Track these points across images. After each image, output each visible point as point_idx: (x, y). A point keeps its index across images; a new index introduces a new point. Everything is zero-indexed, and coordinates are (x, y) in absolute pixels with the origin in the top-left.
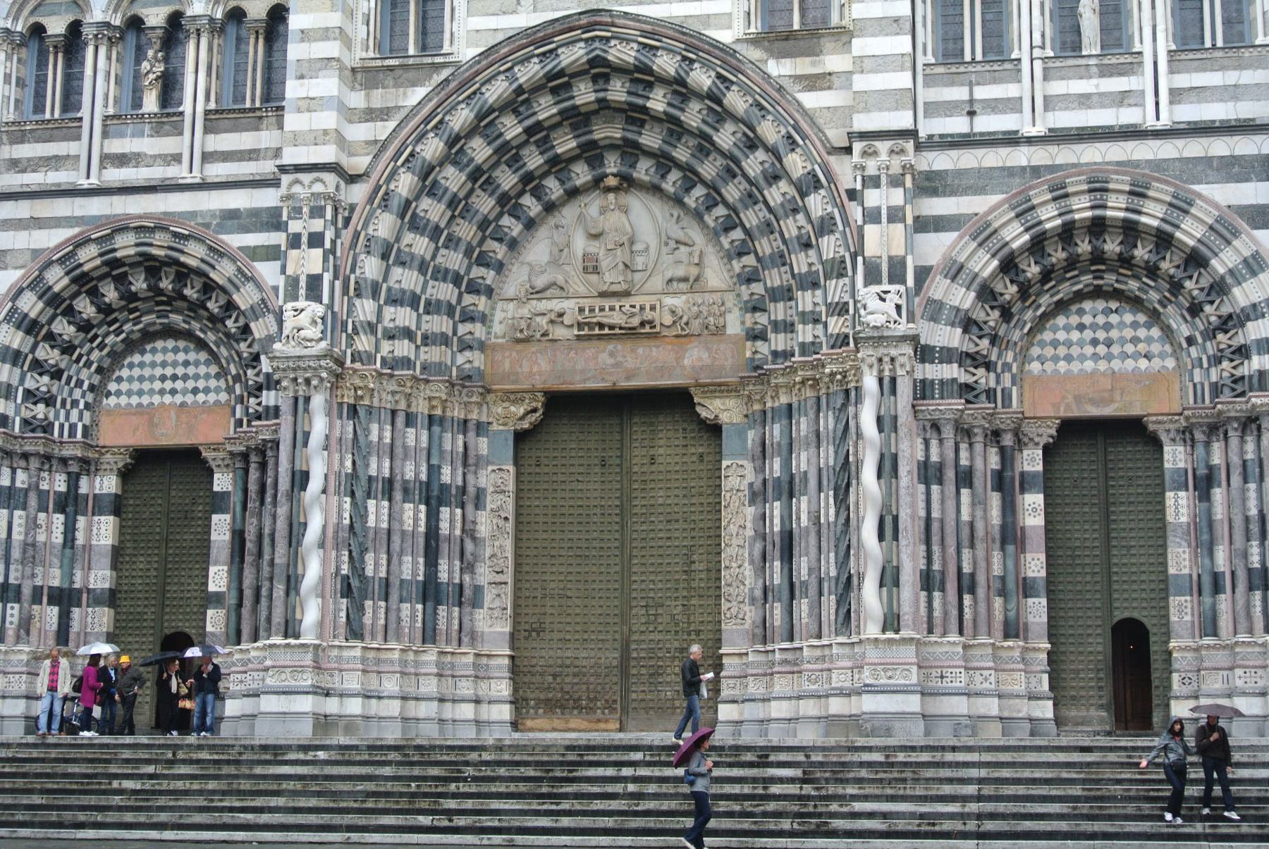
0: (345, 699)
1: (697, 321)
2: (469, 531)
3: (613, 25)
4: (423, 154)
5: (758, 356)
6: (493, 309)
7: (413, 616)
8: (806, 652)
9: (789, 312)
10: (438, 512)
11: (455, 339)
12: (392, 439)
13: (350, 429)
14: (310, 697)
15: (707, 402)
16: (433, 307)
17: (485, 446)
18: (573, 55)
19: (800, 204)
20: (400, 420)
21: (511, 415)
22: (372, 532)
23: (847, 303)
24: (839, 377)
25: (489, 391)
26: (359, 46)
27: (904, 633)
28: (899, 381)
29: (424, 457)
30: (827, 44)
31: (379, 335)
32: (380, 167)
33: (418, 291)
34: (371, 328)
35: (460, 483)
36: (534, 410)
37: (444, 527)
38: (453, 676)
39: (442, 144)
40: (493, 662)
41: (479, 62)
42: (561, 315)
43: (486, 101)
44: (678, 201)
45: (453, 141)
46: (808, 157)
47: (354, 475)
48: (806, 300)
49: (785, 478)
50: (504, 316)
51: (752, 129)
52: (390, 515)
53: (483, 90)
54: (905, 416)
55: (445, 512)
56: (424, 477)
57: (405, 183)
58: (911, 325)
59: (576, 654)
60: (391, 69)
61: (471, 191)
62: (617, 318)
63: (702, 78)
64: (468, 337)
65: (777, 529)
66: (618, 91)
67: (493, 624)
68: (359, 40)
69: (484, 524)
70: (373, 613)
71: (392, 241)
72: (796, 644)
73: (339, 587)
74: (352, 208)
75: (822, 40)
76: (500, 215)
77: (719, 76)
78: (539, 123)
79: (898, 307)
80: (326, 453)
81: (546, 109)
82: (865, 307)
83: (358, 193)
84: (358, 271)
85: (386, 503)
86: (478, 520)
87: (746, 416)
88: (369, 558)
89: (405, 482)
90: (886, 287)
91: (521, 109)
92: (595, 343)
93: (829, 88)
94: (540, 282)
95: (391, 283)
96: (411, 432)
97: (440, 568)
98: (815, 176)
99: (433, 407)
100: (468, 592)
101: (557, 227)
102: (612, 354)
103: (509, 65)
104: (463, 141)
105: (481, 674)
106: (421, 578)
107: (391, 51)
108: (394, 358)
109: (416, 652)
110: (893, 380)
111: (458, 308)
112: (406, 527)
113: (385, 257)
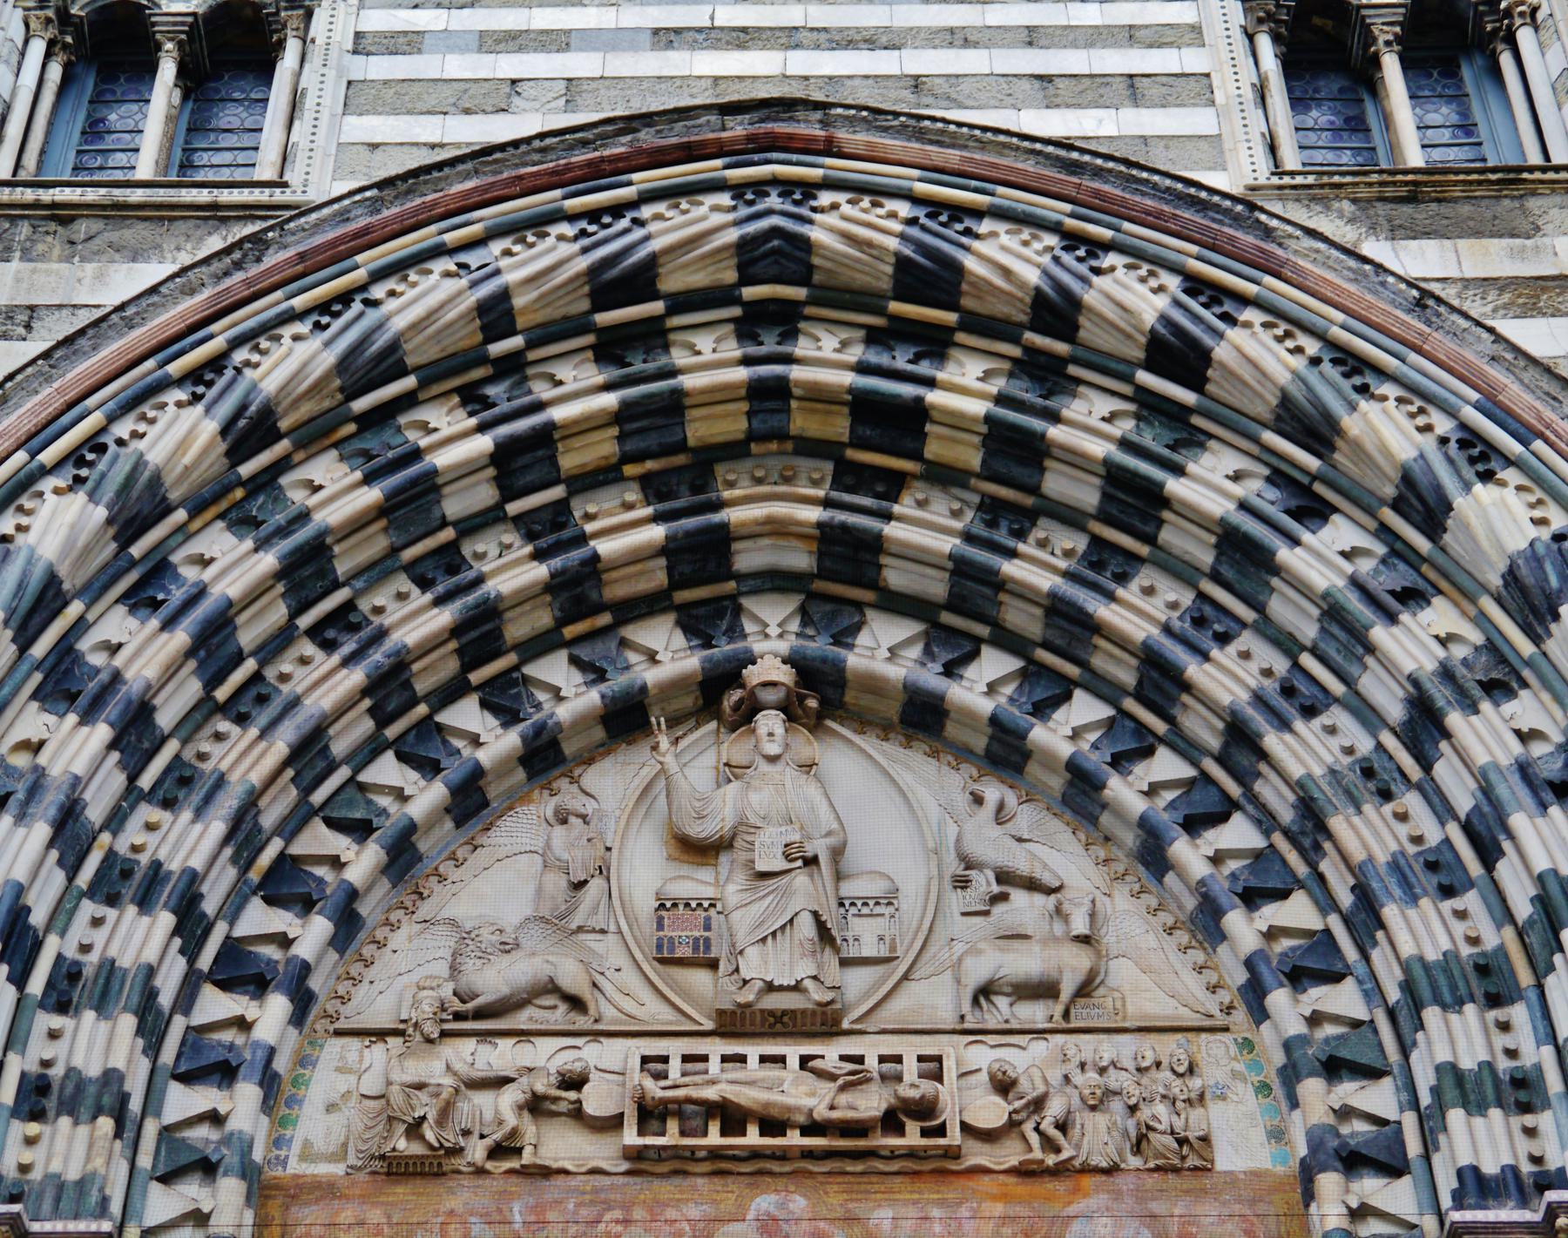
1: (1101, 1120)
3: (830, 148)
6: (303, 1061)
9: (1501, 1041)
11: (151, 1129)
18: (693, 228)
39: (211, 427)
41: (375, 206)
42: (574, 1082)
43: (380, 326)
44: (1005, 752)
45: (250, 431)
60: (62, 215)
64: (203, 1132)
75: (1533, 203)
77: (1195, 285)
78: (546, 437)
81: (577, 392)
91: (492, 391)
94: (494, 979)
103: (476, 229)
111: (178, 1025)
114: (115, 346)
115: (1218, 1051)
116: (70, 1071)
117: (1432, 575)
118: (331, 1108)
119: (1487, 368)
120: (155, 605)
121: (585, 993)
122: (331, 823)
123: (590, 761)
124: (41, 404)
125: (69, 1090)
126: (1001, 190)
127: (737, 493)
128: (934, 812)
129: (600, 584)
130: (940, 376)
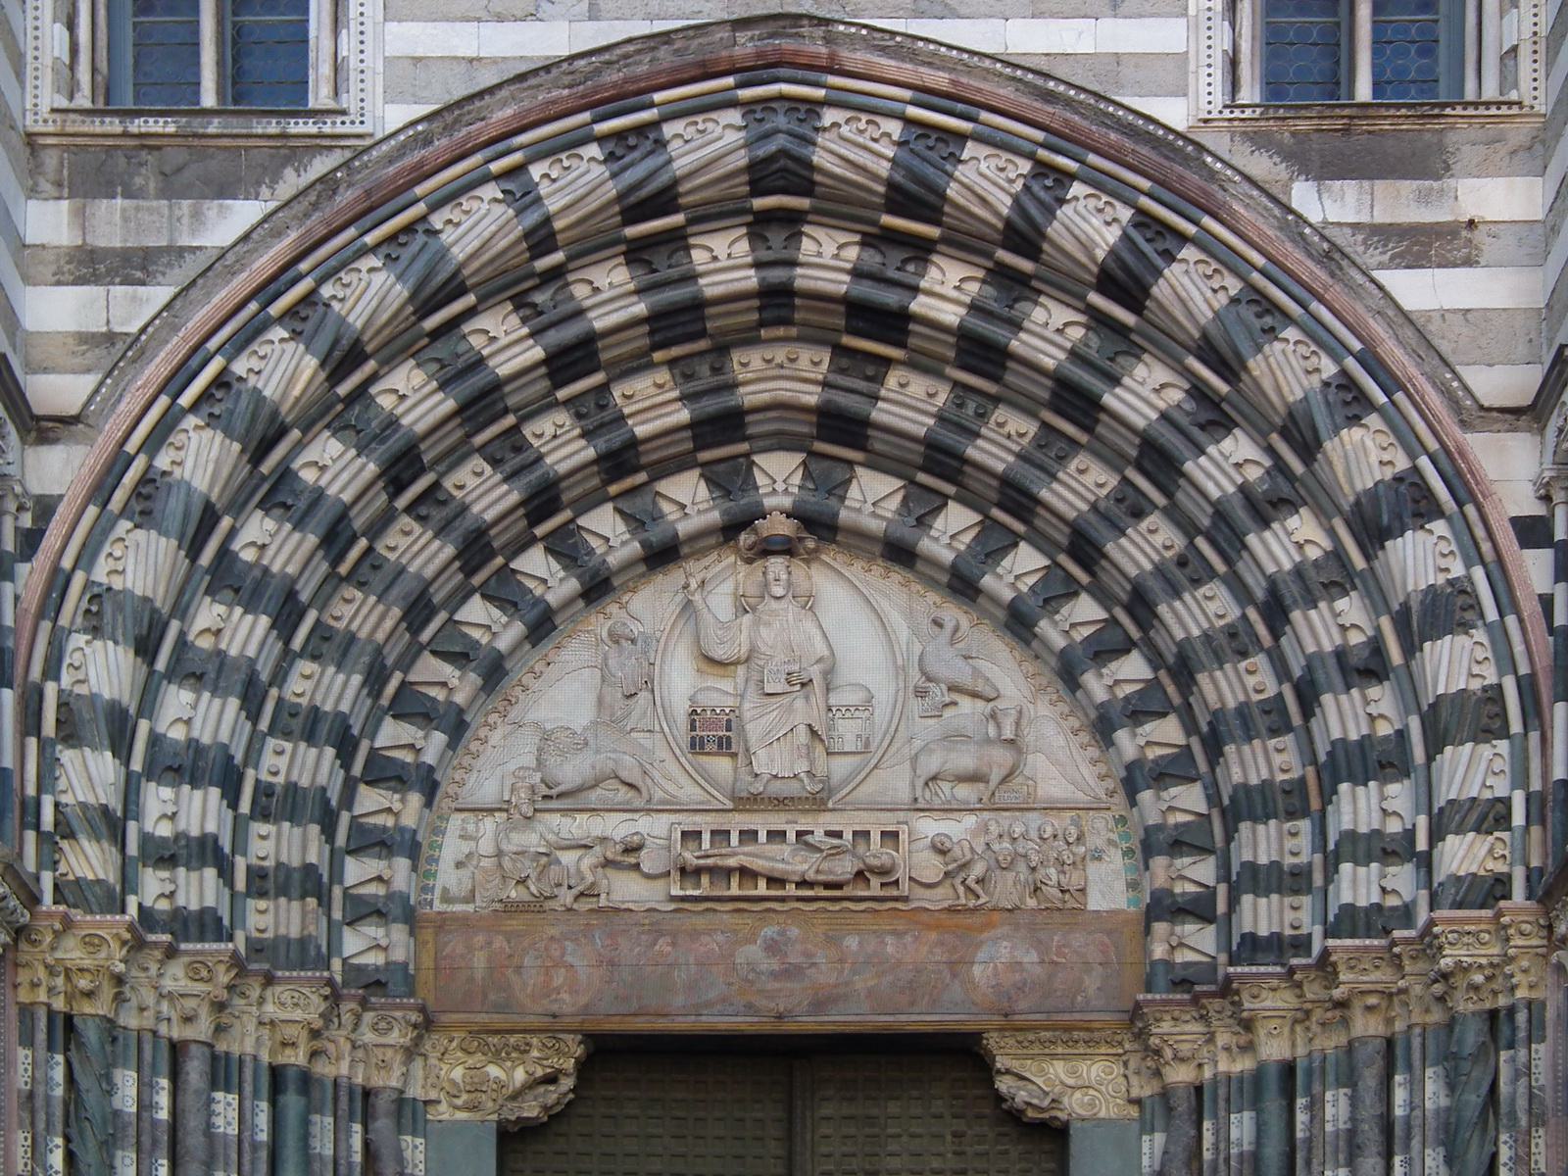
114: (223, 293)
117: (1303, 492)
119: (1371, 321)
120: (287, 507)
123: (634, 591)
124: (171, 352)
125: (282, 878)
129: (638, 455)
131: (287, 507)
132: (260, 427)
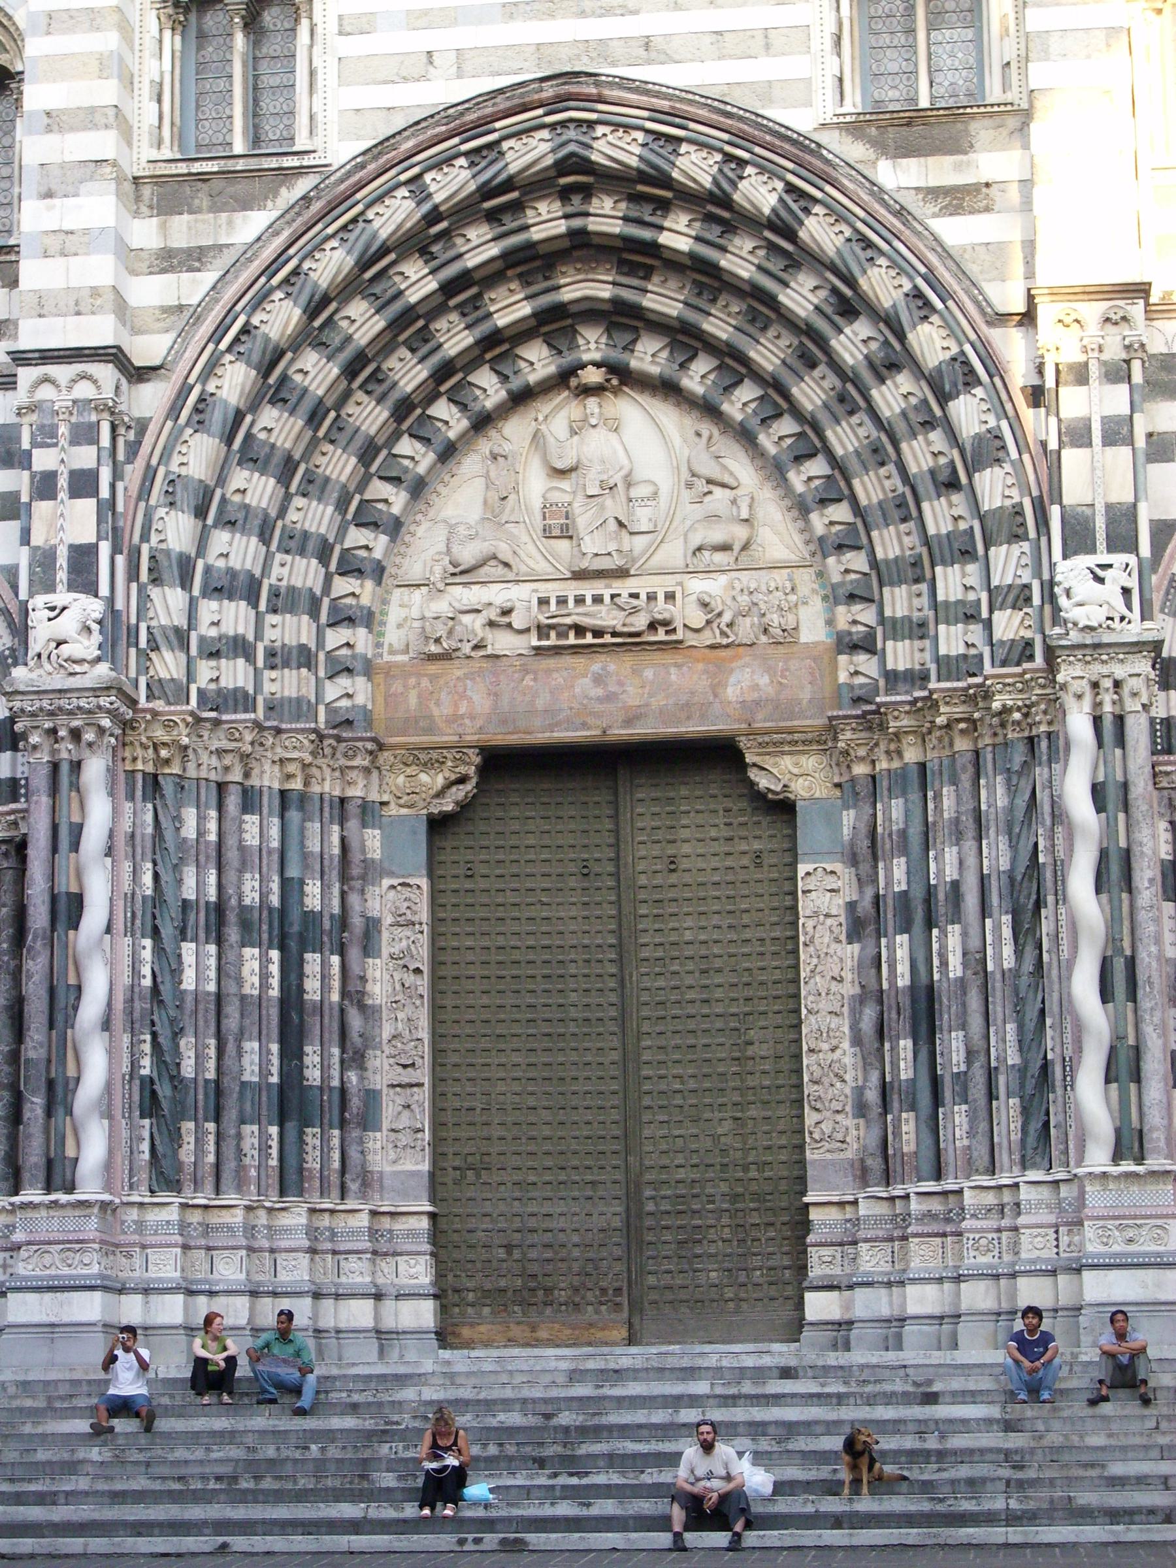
0: (153, 1298)
1: (748, 620)
2: (353, 992)
4: (264, 329)
5: (861, 680)
6: (385, 602)
7: (264, 1148)
8: (969, 1198)
9: (916, 602)
10: (301, 962)
11: (322, 656)
12: (220, 834)
13: (149, 817)
14: (98, 1295)
15: (767, 762)
16: (285, 601)
17: (378, 844)
18: (529, 153)
19: (938, 412)
20: (233, 801)
21: (416, 789)
22: (189, 999)
23: (1027, 587)
24: (1017, 716)
25: (381, 747)
26: (145, 138)
27: (1154, 1163)
28: (1130, 721)
29: (276, 866)
30: (981, 131)
31: (194, 651)
32: (191, 354)
33: (257, 573)
34: (181, 638)
35: (336, 910)
36: (462, 780)
37: (312, 986)
38: (335, 1252)
39: (298, 312)
40: (401, 1225)
41: (362, 166)
43: (374, 236)
44: (709, 410)
46: (952, 330)
47: (158, 898)
48: (952, 582)
49: (918, 894)
50: (405, 616)
51: (851, 282)
52: (219, 969)
53: (370, 215)
54: (1141, 786)
55: (313, 961)
56: (275, 900)
57: (234, 381)
58: (1148, 624)
59: (547, 1208)
60: (203, 178)
61: (346, 395)
62: (607, 617)
63: (760, 193)
65: (903, 981)
66: (607, 216)
67: (398, 1153)
68: (145, 128)
69: (379, 980)
70: (195, 1144)
71: (212, 484)
72: (949, 1184)
73: (136, 1097)
74: (142, 426)
75: (974, 126)
76: (396, 436)
77: (791, 188)
79: (1126, 591)
80: (109, 860)
82: (1068, 593)
83: (149, 400)
84: (154, 538)
85: (212, 949)
86: (369, 975)
87: (838, 785)
88: (187, 1044)
89: (243, 909)
90: (1104, 558)
91: (435, 249)
92: (568, 660)
93: (987, 209)
94: (468, 554)
95: (212, 557)
96: (251, 821)
97: (307, 1060)
98: (966, 363)
99: (289, 777)
100: (355, 1103)
101: (494, 457)
102: (598, 680)
103: (416, 170)
104: (334, 305)
105: (383, 1247)
106: (275, 1079)
107: (199, 146)
108: (219, 691)
109: (270, 1210)
110: (1120, 720)
111: (326, 602)
112: (247, 990)
113: (201, 512)
115: (806, 577)
116: (284, 645)
118: (399, 626)
120: (285, 401)
121: (512, 563)
122: (381, 478)
126: (692, 125)
127: (568, 280)
128: (677, 441)
130: (666, 224)
131: (285, 401)
132: (268, 357)
